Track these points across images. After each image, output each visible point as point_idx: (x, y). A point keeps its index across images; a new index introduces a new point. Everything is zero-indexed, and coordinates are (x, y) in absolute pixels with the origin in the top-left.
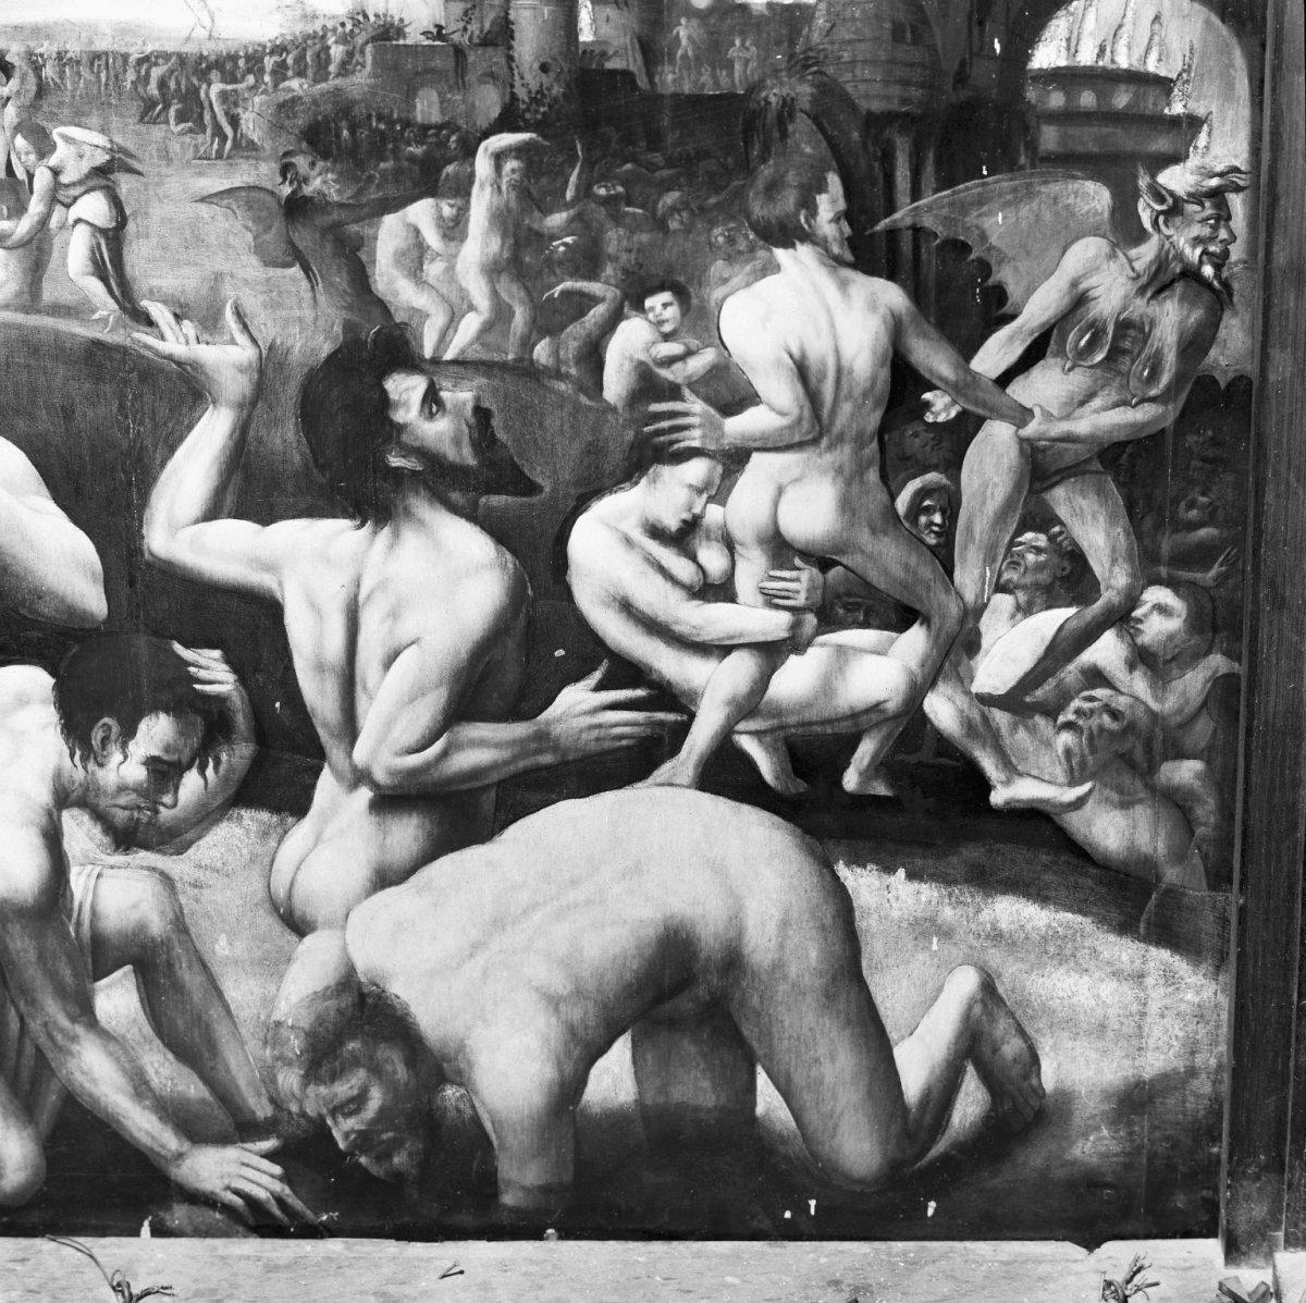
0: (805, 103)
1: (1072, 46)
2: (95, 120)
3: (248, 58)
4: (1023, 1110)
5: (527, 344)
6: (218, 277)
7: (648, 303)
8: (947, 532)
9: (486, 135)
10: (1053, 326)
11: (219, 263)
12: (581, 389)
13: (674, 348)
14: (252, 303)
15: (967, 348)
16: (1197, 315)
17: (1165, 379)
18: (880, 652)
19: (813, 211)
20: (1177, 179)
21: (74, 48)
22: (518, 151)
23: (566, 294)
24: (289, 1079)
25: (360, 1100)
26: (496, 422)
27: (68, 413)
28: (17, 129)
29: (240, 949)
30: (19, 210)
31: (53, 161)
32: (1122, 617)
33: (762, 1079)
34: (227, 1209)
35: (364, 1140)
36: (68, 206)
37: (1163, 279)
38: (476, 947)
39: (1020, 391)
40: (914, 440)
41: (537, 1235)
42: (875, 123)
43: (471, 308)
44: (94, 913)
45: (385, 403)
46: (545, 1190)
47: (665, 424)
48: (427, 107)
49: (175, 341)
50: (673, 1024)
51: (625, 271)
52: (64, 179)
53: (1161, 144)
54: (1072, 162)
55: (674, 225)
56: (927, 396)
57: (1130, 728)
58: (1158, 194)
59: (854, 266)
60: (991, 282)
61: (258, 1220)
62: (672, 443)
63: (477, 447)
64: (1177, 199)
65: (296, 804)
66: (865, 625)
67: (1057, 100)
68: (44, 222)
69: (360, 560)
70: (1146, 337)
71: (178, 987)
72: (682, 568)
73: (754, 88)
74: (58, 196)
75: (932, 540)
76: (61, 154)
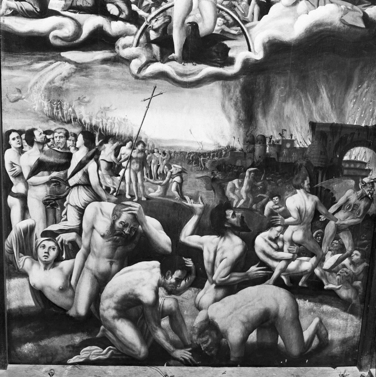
0: (304, 164)
1: (350, 156)
2: (180, 163)
3: (208, 153)
4: (325, 343)
5: (252, 205)
6: (198, 192)
7: (273, 198)
8: (321, 240)
9: (248, 168)
10: (342, 205)
11: (199, 189)
12: (260, 213)
13: (277, 206)
14: (204, 196)
15: (328, 208)
16: (367, 203)
17: (361, 214)
18: (308, 261)
19: (304, 183)
20: (366, 180)
21: (177, 151)
22: (253, 171)
23: (259, 196)
24: (195, 337)
25: (207, 341)
26: (245, 219)
27: (168, 215)
28: (165, 165)
29: (189, 313)
30: (164, 179)
31: (171, 170)
32: (349, 256)
33: (279, 337)
34: (181, 361)
35: (207, 349)
36: (173, 179)
37: (362, 197)
38: (231, 313)
39: (336, 216)
40: (317, 224)
41: (236, 366)
42: (316, 168)
43: (243, 198)
44: (163, 306)
45: (225, 215)
46: (238, 358)
47: (274, 220)
48: (238, 163)
49: (189, 203)
50: (265, 327)
51: (270, 193)
52: (173, 174)
53: (364, 174)
54: (349, 176)
55: (279, 185)
56: (320, 216)
57: (349, 275)
58: (363, 182)
59: (310, 193)
60: (333, 196)
61: (186, 363)
62: (275, 223)
63: (241, 223)
64: (366, 183)
65: (202, 287)
66: (306, 256)
67: (347, 166)
68: (168, 181)
69: (218, 243)
70: (358, 207)
71: (177, 320)
72: (274, 245)
73: (295, 162)
74: (172, 177)
75: (319, 242)
76: (173, 169)
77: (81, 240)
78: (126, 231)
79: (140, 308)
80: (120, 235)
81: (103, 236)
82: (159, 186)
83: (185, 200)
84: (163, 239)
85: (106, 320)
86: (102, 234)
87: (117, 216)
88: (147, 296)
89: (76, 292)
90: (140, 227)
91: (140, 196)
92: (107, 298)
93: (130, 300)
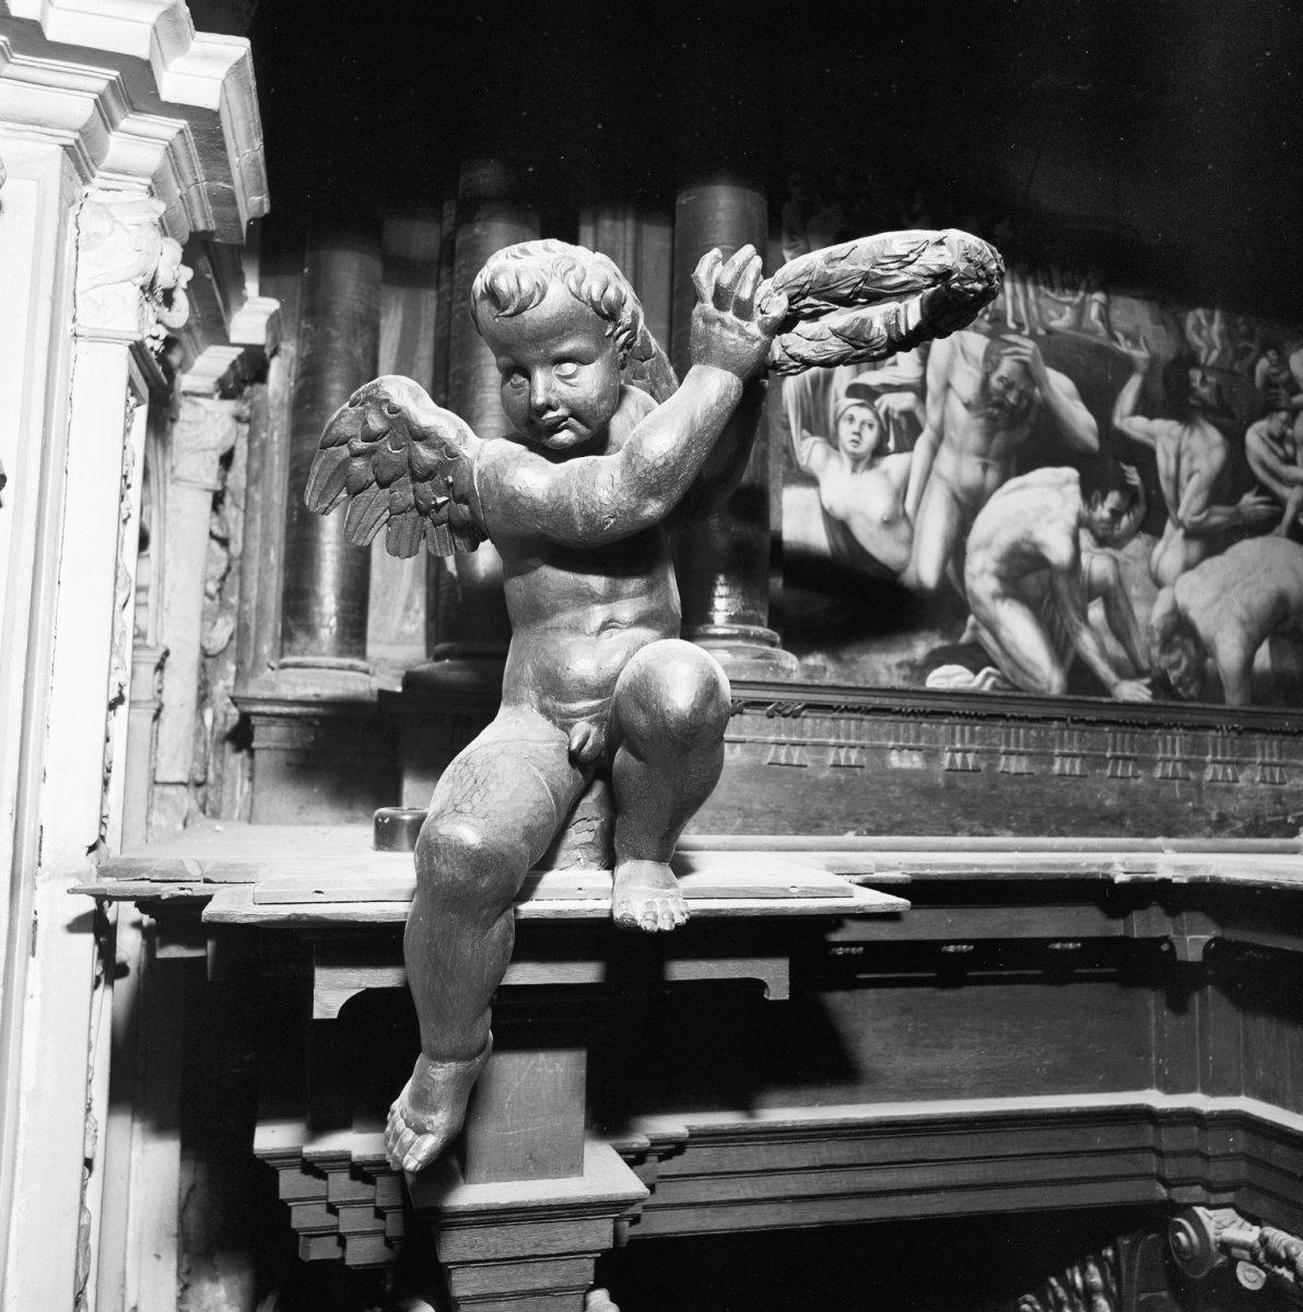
5: (1232, 364)
14: (1149, 337)
24: (1155, 651)
35: (1180, 681)
45: (1188, 380)
49: (1124, 347)
65: (1157, 533)
69: (1180, 438)
71: (1118, 607)
72: (1281, 452)
77: (924, 411)
78: (1012, 398)
79: (1044, 574)
80: (998, 405)
81: (967, 406)
82: (1068, 309)
83: (1116, 339)
84: (1081, 419)
85: (978, 602)
86: (966, 401)
87: (993, 365)
88: (1058, 550)
89: (917, 528)
90: (1037, 391)
91: (1034, 326)
92: (978, 548)
93: (1025, 555)
